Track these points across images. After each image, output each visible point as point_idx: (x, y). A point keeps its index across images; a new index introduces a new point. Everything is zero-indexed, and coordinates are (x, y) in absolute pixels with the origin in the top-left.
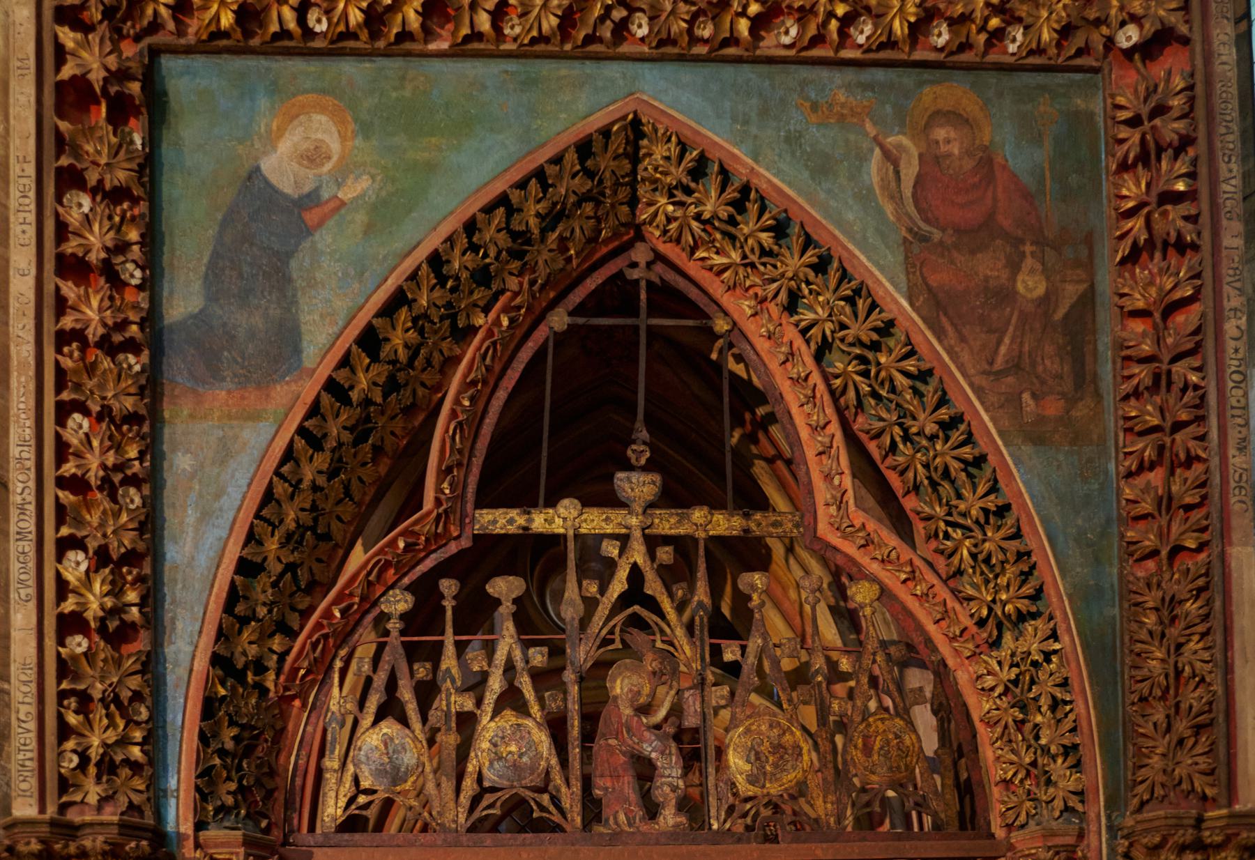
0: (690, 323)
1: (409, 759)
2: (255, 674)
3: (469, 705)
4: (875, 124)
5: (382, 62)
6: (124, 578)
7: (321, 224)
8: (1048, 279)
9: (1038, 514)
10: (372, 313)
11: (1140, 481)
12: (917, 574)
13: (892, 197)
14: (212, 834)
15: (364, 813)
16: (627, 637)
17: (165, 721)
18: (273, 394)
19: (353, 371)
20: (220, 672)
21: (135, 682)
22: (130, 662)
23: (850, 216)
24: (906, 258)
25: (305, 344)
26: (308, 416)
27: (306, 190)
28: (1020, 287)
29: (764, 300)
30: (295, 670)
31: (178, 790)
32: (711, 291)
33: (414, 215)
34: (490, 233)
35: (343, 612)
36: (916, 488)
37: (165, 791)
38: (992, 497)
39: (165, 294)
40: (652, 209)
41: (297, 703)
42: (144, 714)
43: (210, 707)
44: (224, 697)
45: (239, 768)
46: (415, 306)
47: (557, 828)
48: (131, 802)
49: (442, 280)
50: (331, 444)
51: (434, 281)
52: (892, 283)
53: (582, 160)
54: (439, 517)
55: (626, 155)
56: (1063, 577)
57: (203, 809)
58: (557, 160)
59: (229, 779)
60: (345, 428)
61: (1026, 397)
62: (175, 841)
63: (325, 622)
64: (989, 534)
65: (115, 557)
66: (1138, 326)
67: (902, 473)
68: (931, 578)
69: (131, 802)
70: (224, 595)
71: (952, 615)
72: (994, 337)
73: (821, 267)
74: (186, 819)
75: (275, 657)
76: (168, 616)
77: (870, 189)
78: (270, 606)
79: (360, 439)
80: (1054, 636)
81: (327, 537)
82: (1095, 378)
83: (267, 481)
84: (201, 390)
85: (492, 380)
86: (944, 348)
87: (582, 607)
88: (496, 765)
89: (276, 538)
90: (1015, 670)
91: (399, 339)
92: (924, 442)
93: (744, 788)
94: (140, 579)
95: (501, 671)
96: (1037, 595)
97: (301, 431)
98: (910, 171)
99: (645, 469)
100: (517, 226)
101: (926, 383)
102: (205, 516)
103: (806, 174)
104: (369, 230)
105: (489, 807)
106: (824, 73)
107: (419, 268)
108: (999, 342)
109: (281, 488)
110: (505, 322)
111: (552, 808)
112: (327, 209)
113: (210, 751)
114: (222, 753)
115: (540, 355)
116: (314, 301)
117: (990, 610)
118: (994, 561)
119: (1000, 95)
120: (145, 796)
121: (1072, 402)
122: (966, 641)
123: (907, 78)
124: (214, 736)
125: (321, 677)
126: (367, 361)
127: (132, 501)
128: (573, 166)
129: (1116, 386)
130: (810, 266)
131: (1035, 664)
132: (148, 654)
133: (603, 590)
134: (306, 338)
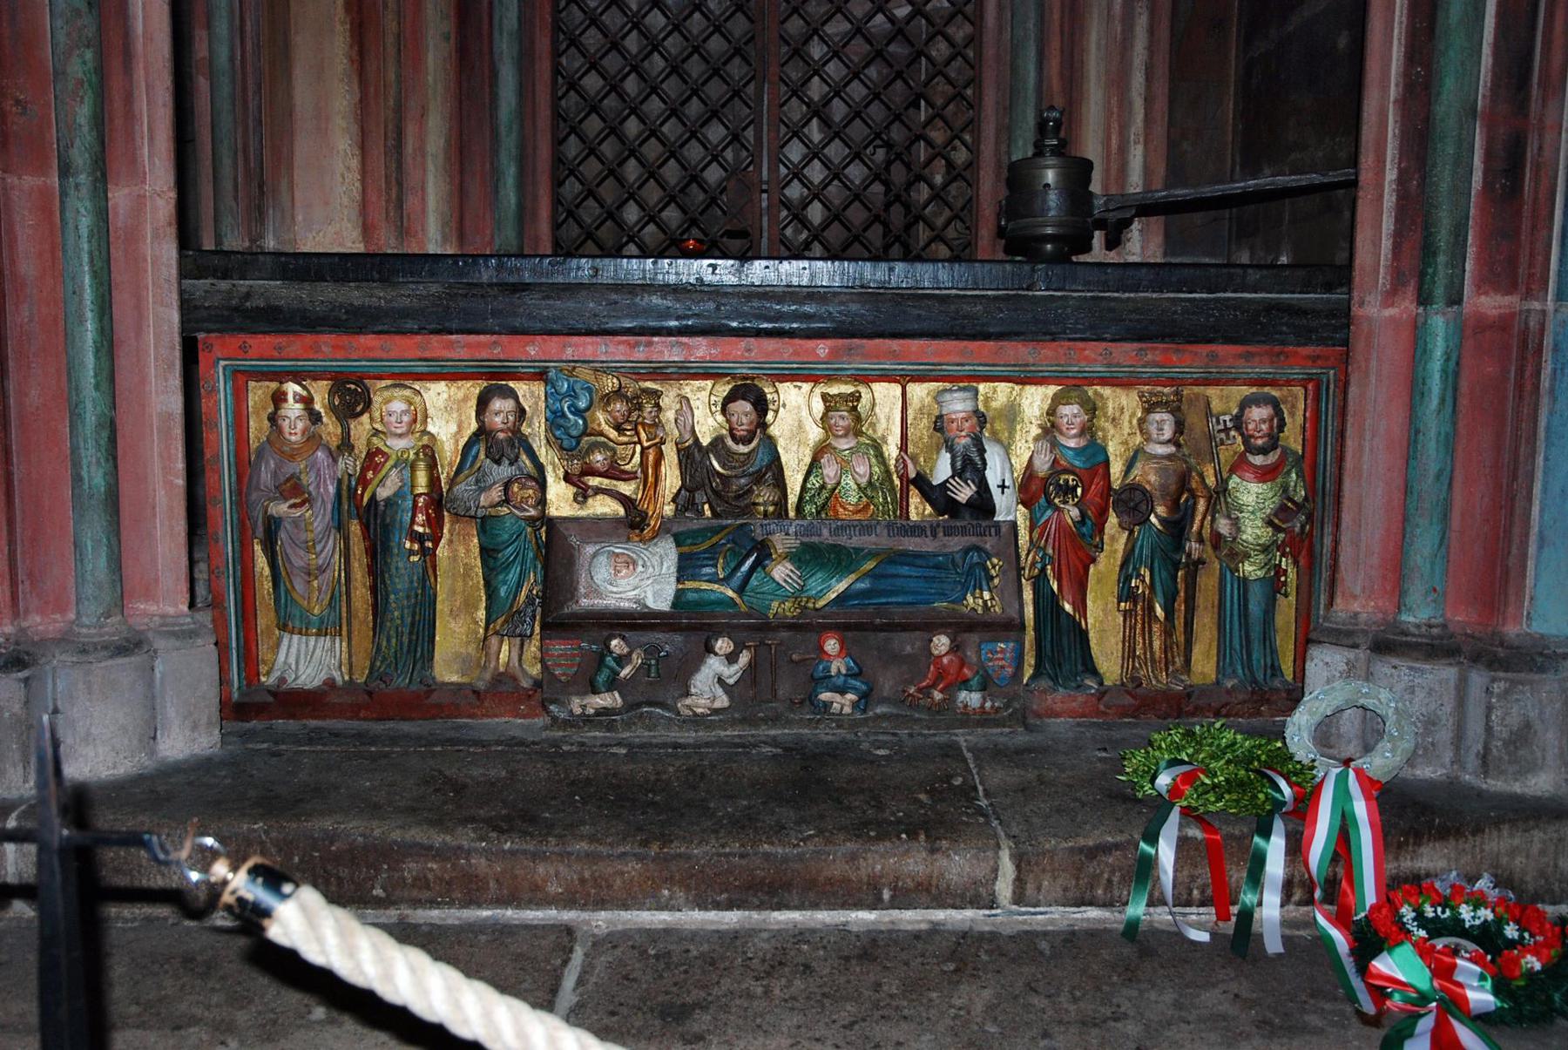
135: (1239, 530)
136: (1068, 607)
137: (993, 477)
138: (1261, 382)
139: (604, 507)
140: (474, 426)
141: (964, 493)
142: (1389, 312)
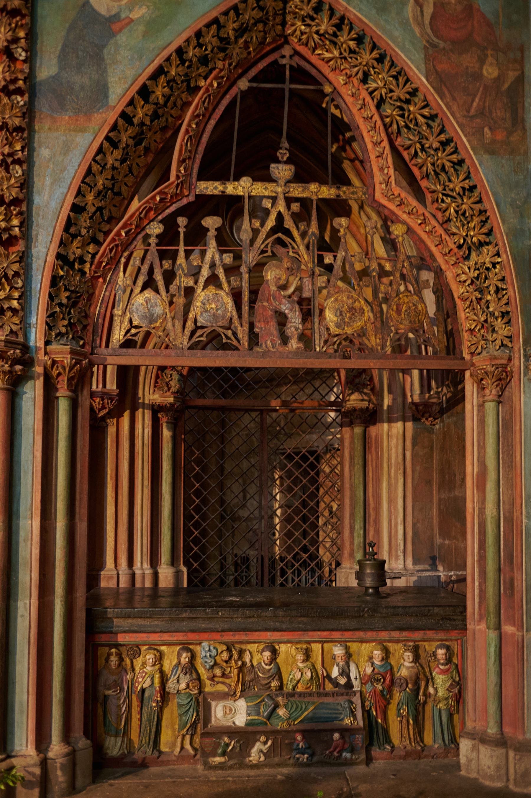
0: (312, 87)
1: (158, 310)
2: (79, 264)
6: (11, 212)
7: (121, 30)
8: (499, 69)
9: (491, 191)
10: (146, 78)
12: (427, 220)
13: (419, 24)
14: (54, 347)
15: (134, 338)
16: (275, 250)
17: (31, 288)
18: (93, 119)
19: (135, 108)
20: (61, 263)
21: (16, 267)
22: (13, 256)
23: (397, 34)
24: (426, 56)
25: (110, 93)
26: (111, 131)
27: (113, 13)
28: (485, 72)
29: (350, 76)
31: (36, 324)
32: (323, 71)
33: (169, 27)
34: (209, 38)
35: (126, 233)
36: (428, 176)
37: (30, 324)
38: (467, 181)
39: (38, 65)
40: (293, 28)
41: (101, 280)
42: (20, 284)
43: (54, 281)
44: (62, 276)
45: (69, 313)
46: (168, 75)
48: (11, 330)
49: (183, 62)
50: (122, 145)
51: (179, 62)
52: (418, 69)
54: (178, 185)
56: (503, 224)
57: (50, 334)
59: (64, 318)
60: (130, 137)
61: (486, 129)
62: (34, 351)
63: (117, 238)
64: (465, 200)
65: (7, 201)
67: (420, 168)
68: (434, 223)
69: (11, 330)
70: (64, 222)
71: (444, 242)
73: (380, 59)
74: (40, 339)
75: (90, 256)
76: (34, 233)
77: (408, 20)
78: (88, 229)
79: (138, 143)
80: (498, 254)
81: (119, 194)
83: (88, 164)
84: (55, 115)
85: (207, 115)
86: (444, 104)
87: (251, 233)
88: (204, 315)
89: (92, 193)
90: (477, 272)
92: (432, 152)
93: (334, 330)
94: (20, 213)
95: (208, 266)
96: (489, 233)
97: (107, 138)
99: (286, 162)
100: (223, 35)
101: (434, 121)
102: (55, 181)
103: (374, 12)
104: (145, 35)
107: (171, 55)
108: (473, 101)
109: (96, 168)
110: (215, 85)
112: (123, 23)
113: (54, 304)
114: (60, 305)
115: (233, 102)
116: (116, 71)
117: (465, 240)
118: (467, 215)
120: (19, 326)
121: (510, 133)
122: (452, 256)
124: (56, 296)
125: (113, 267)
126: (143, 103)
127: (17, 172)
128: (253, 4)
130: (376, 59)
131: (488, 269)
132: (23, 252)
133: (262, 225)
134: (111, 90)
135: (437, 692)
136: (380, 721)
137: (353, 675)
138: (442, 640)
139: (221, 688)
140: (175, 661)
141: (343, 681)
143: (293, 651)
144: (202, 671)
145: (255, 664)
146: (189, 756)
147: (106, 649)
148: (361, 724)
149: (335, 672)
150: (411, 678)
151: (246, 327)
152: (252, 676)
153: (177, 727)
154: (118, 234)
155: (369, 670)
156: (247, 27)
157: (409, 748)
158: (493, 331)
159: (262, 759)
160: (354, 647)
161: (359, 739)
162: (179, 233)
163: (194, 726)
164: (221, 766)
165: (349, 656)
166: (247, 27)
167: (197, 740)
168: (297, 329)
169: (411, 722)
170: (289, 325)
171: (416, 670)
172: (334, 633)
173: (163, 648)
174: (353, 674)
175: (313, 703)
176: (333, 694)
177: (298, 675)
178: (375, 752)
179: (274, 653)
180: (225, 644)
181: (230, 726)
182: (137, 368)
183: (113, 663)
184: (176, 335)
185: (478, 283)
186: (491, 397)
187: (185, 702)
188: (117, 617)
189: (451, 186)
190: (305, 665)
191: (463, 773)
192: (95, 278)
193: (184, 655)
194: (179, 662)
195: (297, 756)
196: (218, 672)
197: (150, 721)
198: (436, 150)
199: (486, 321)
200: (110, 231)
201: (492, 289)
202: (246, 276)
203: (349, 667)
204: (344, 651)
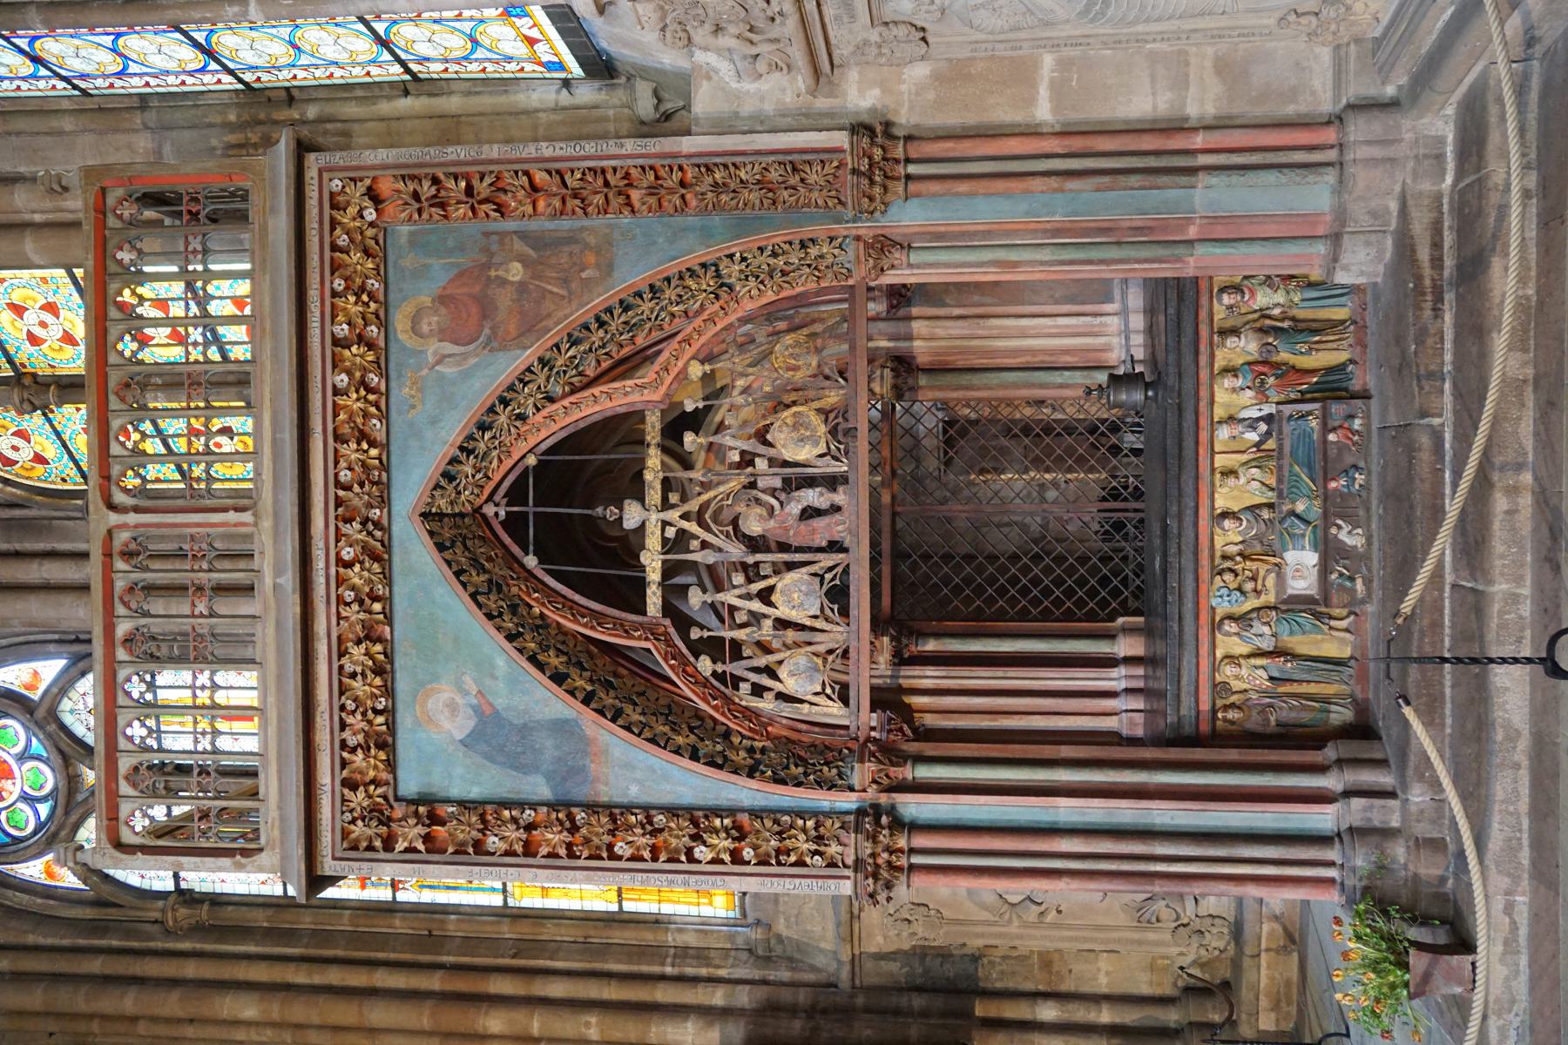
3: (768, 624)
4: (422, 369)
5: (397, 665)
11: (637, 205)
13: (465, 359)
19: (576, 688)
23: (477, 385)
28: (517, 278)
30: (751, 729)
35: (715, 699)
47: (846, 571)
49: (520, 634)
53: (448, 548)
55: (441, 521)
56: (694, 252)
58: (449, 563)
61: (584, 275)
66: (541, 204)
72: (548, 296)
80: (731, 256)
81: (669, 706)
82: (569, 231)
91: (555, 661)
93: (822, 449)
96: (704, 265)
98: (449, 348)
100: (485, 590)
105: (832, 610)
106: (392, 400)
108: (551, 292)
111: (834, 572)
119: (401, 290)
121: (587, 246)
123: (393, 348)
129: (579, 218)
137: (1258, 414)
139: (1271, 581)
140: (1235, 639)
141: (1263, 427)
142: (1192, 263)
143: (1224, 490)
144: (1248, 606)
145: (1241, 539)
146: (1355, 622)
147: (1219, 723)
148: (1317, 405)
149: (1253, 437)
150: (1260, 339)
151: (820, 556)
152: (1255, 542)
153: (1319, 637)
154: (715, 708)
155: (1249, 393)
156: (471, 559)
157: (1351, 341)
158: (822, 257)
159: (1359, 531)
160: (1219, 412)
161: (1338, 409)
162: (709, 637)
163: (1318, 616)
164: (1368, 582)
165: (1231, 419)
166: (471, 559)
167: (1336, 612)
168: (821, 494)
169: (1317, 338)
170: (817, 504)
171: (1251, 335)
172: (1201, 440)
173: (1219, 654)
174: (1254, 413)
175: (1291, 465)
176: (1280, 439)
177: (1255, 484)
178: (1356, 385)
179: (1225, 515)
180: (1212, 578)
181: (1319, 571)
182: (873, 689)
183: (1236, 716)
184: (832, 640)
185: (762, 276)
186: (904, 258)
187: (1287, 626)
188: (1179, 710)
189: (647, 312)
190: (1241, 475)
191: (1379, 280)
192: (769, 737)
193: (1227, 628)
194: (1237, 634)
195: (1357, 487)
196: (1249, 586)
197: (1311, 670)
198: (606, 332)
199: (809, 266)
200: (712, 717)
201: (772, 261)
202: (759, 557)
203: (1245, 420)
204: (1225, 426)
